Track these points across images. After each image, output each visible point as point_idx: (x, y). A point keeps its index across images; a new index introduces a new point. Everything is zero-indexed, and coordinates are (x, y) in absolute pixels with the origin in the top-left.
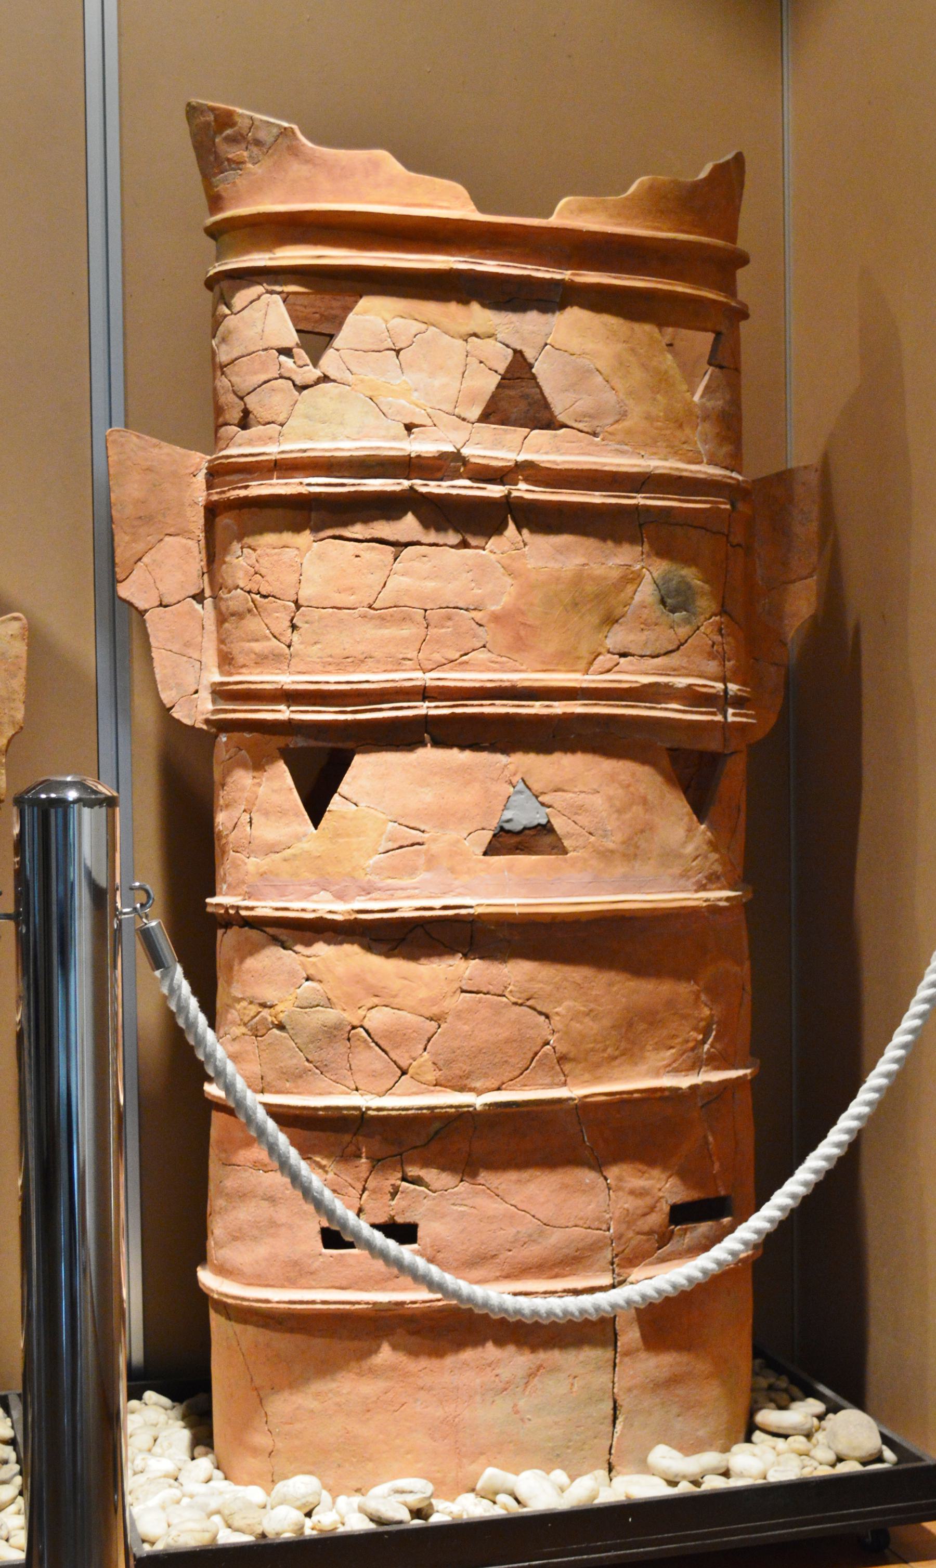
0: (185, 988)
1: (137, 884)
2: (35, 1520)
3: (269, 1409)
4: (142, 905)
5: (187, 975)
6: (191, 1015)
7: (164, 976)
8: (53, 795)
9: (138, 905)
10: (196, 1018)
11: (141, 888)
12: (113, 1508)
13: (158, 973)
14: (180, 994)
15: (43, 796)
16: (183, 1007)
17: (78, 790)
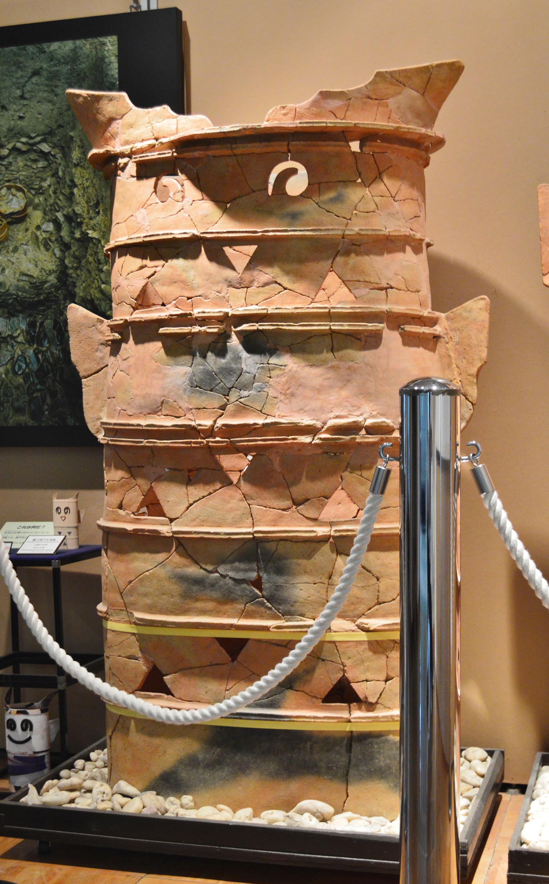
0: (499, 505)
1: (474, 442)
2: (404, 820)
3: (351, 789)
4: (474, 455)
5: (500, 497)
6: (502, 522)
7: (486, 496)
8: (422, 388)
9: (471, 455)
10: (505, 524)
11: (475, 445)
12: (448, 818)
13: (482, 496)
14: (495, 509)
15: (416, 388)
16: (496, 517)
17: (437, 386)
